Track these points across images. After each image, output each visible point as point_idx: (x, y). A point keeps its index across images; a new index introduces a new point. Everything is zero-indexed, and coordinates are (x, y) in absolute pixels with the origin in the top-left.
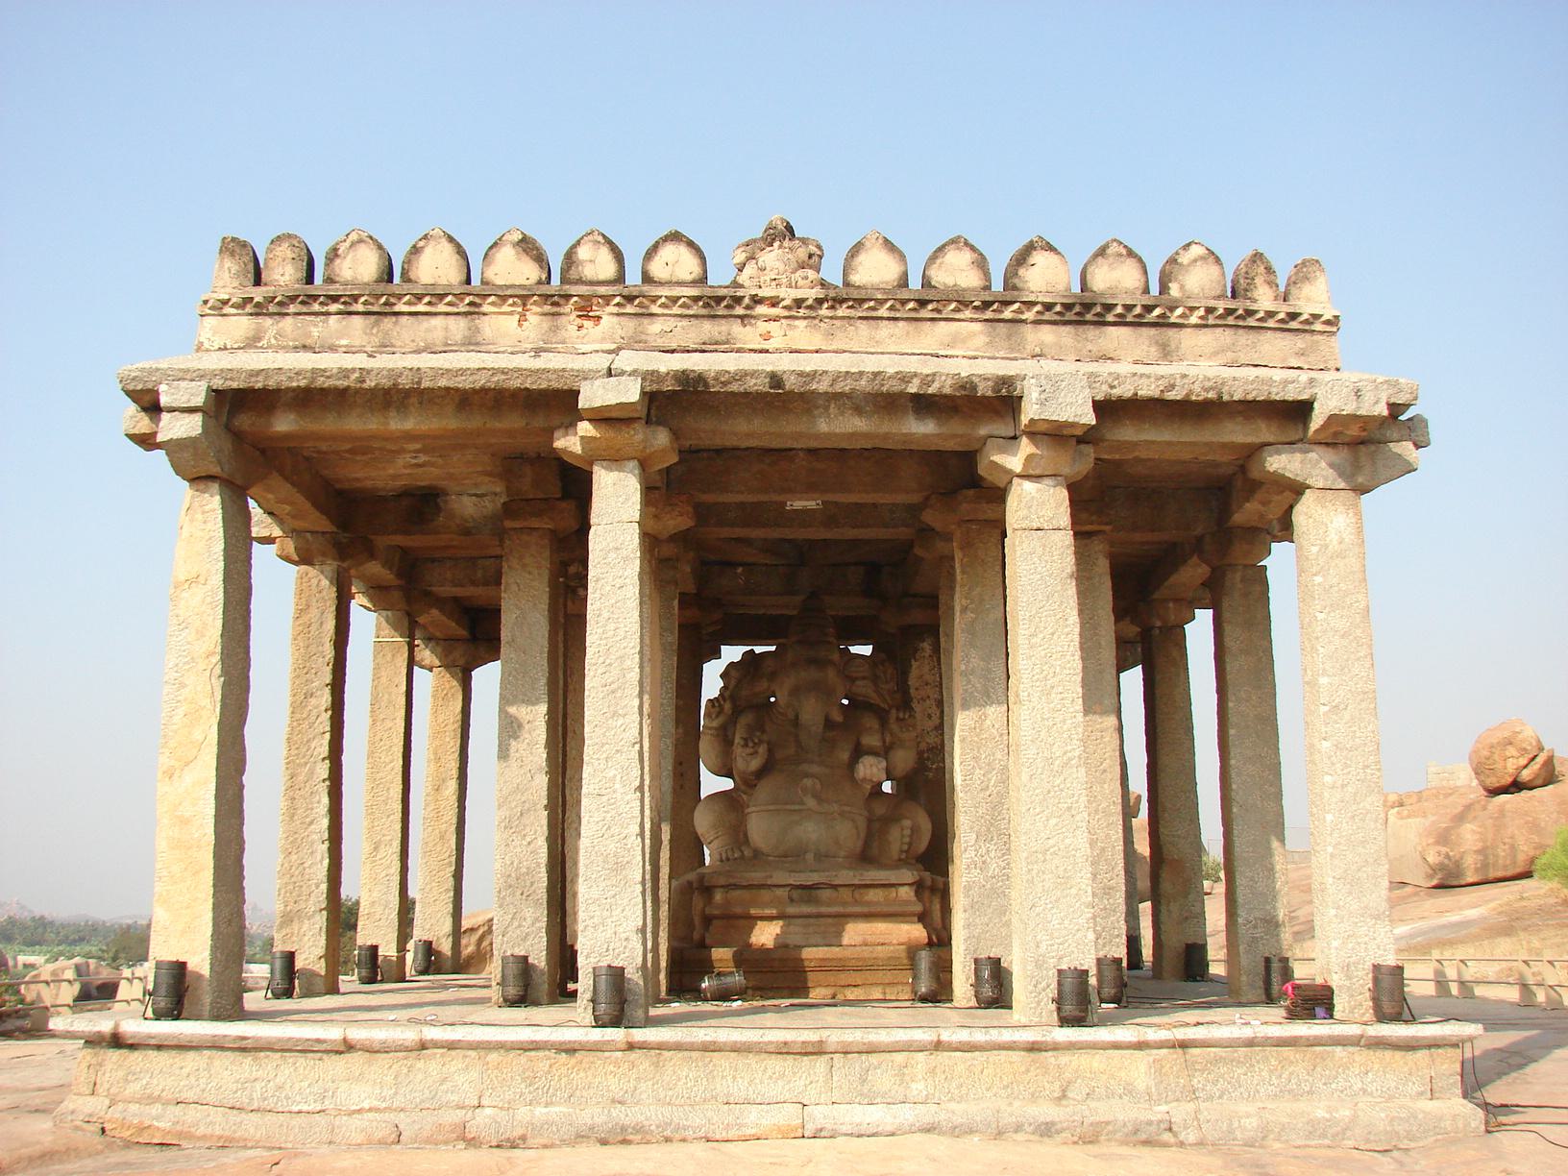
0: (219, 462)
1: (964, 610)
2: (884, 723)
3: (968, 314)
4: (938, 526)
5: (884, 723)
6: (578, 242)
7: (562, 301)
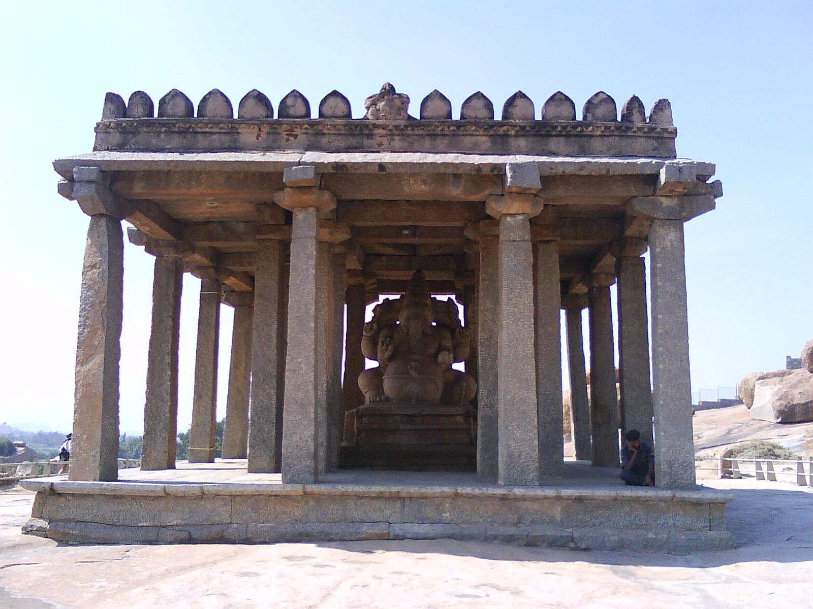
0: (105, 208)
1: (484, 280)
3: (482, 132)
4: (472, 238)
6: (287, 96)
7: (278, 127)
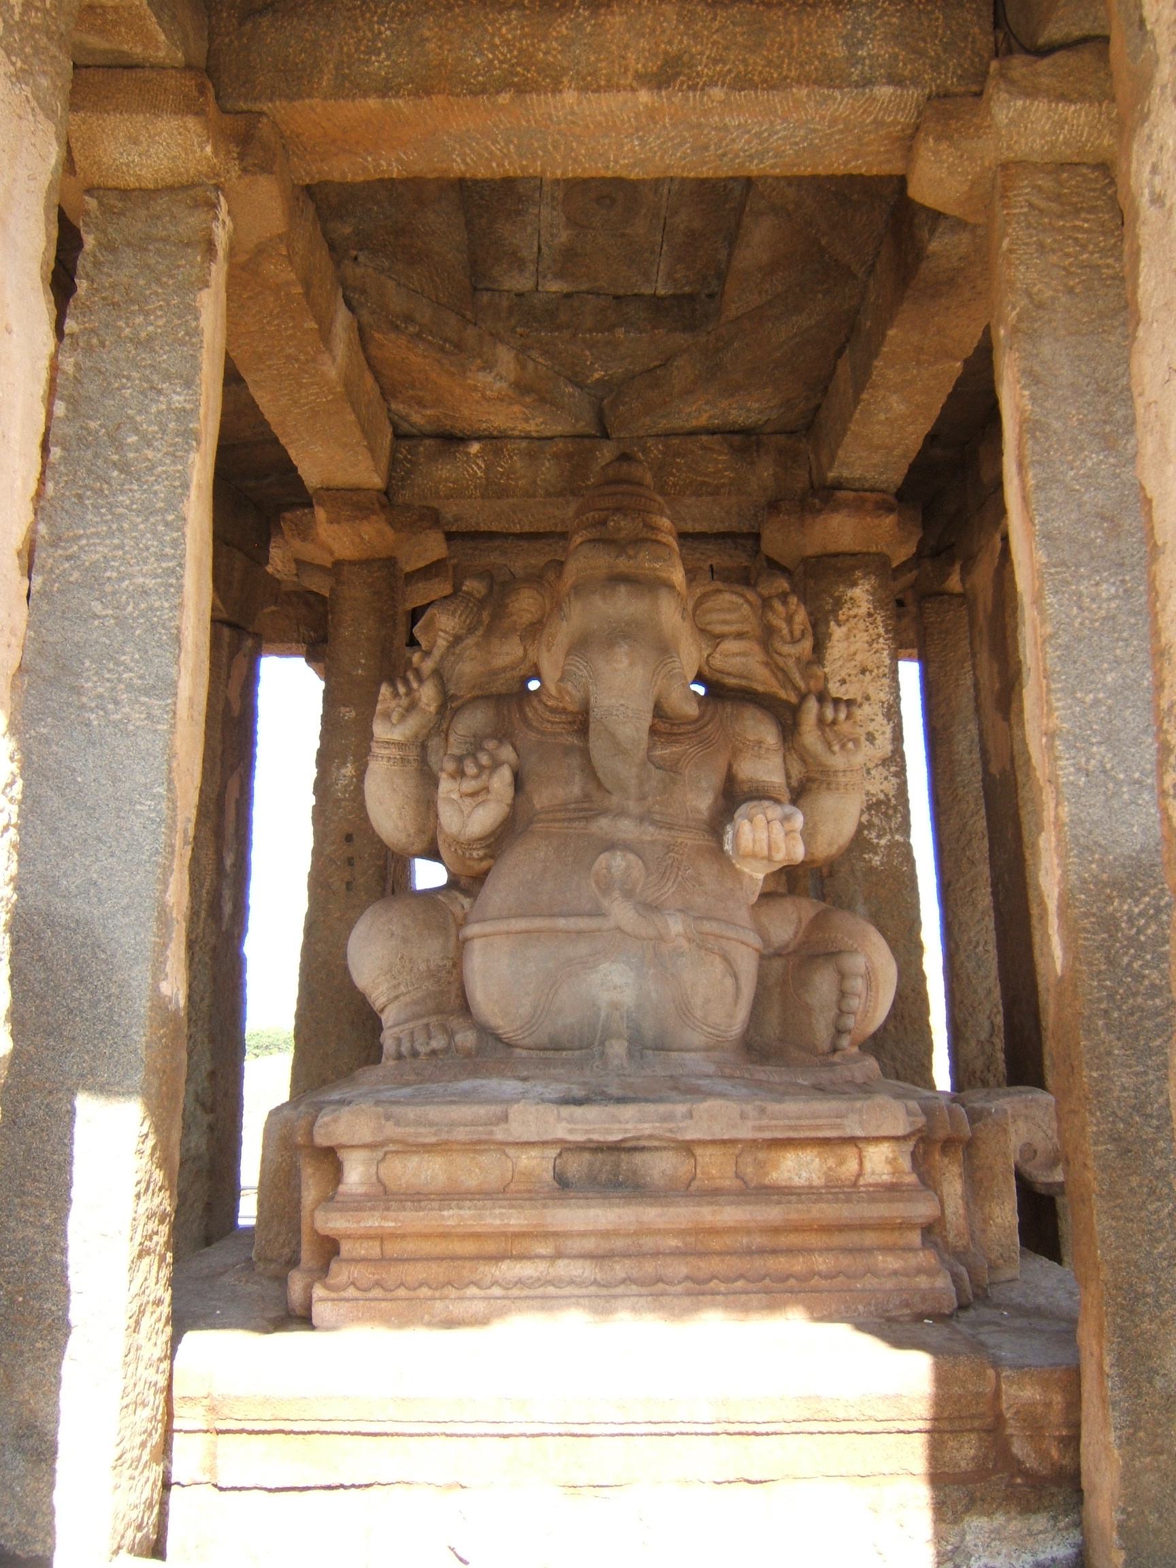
2: (789, 728)
5: (789, 728)
